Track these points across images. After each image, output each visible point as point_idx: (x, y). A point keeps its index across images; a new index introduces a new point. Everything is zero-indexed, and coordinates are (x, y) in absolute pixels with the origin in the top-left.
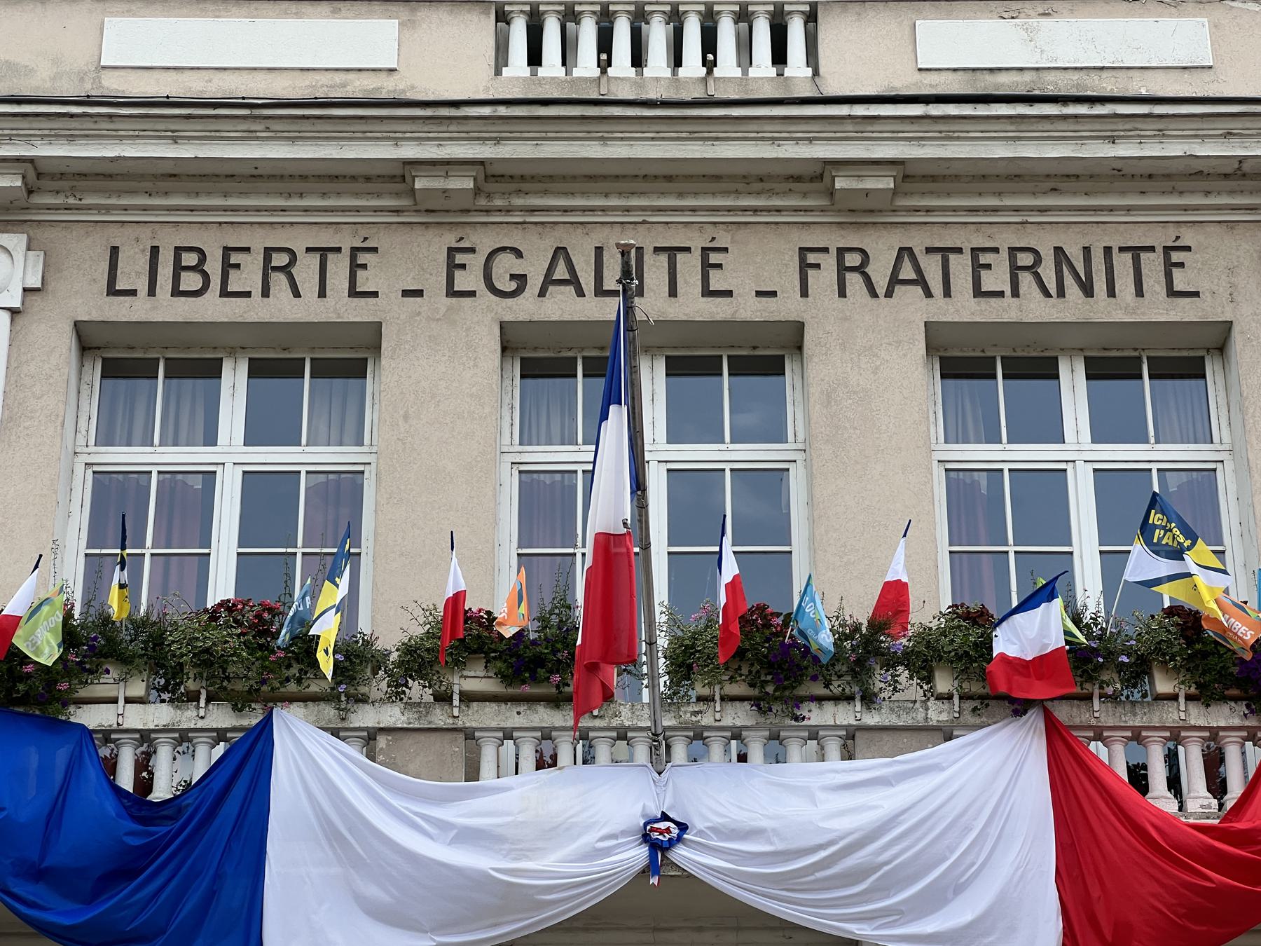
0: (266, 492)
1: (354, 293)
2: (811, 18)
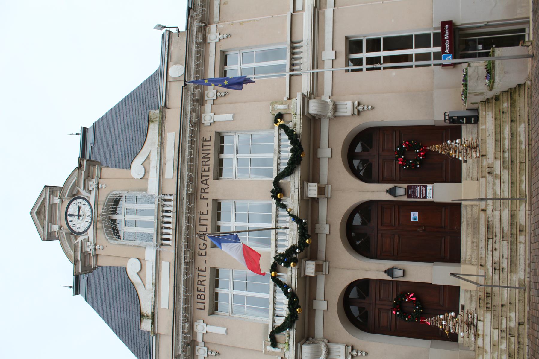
1: (205, 271)
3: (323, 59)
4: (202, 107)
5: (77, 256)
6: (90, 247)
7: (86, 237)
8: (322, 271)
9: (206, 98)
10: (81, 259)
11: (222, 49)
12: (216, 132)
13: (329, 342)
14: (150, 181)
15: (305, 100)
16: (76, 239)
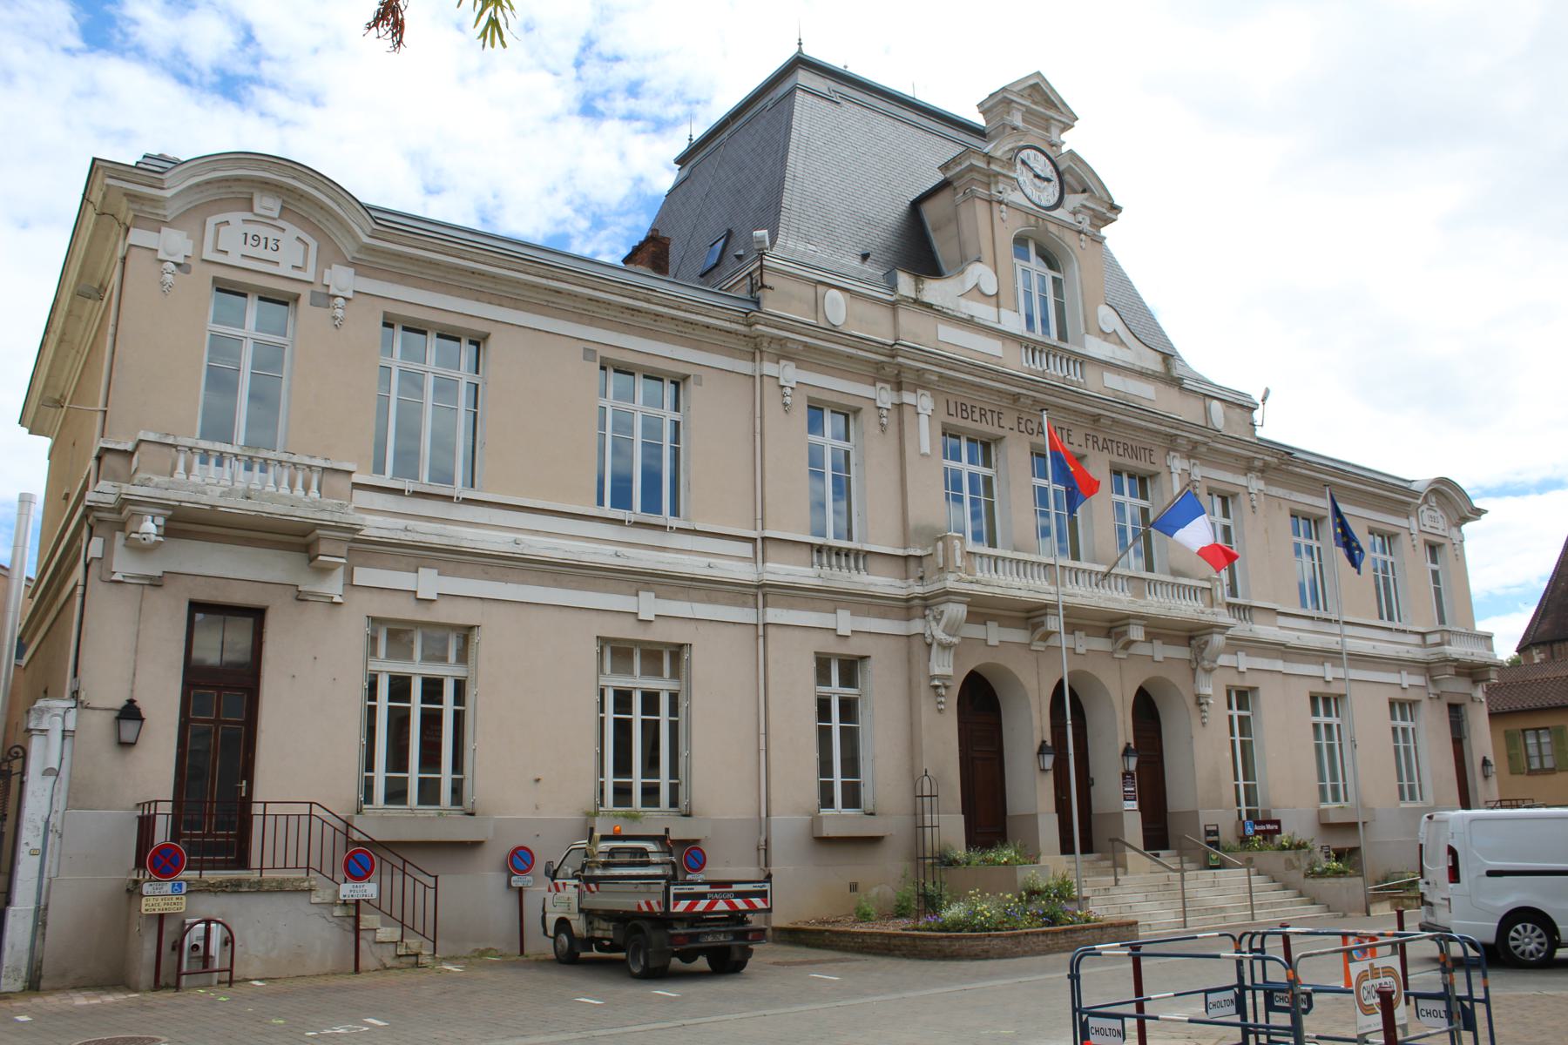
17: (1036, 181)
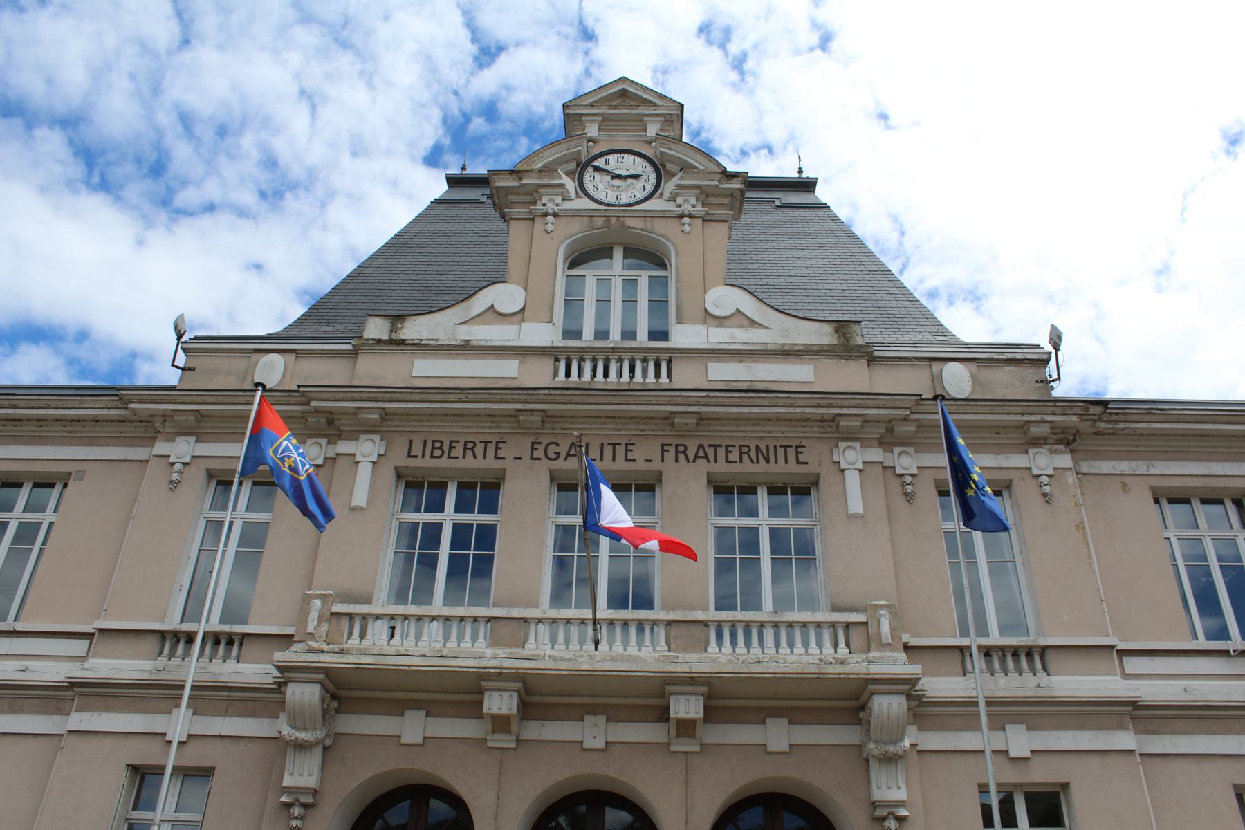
0: (461, 532)
1: (496, 458)
2: (669, 362)
3: (1007, 727)
4: (876, 443)
5: (529, 177)
6: (550, 202)
7: (573, 195)
8: (494, 732)
9: (897, 450)
10: (524, 185)
11: (1015, 483)
12: (818, 475)
13: (325, 748)
14: (701, 328)
15: (907, 686)
16: (568, 174)
17: (617, 182)
